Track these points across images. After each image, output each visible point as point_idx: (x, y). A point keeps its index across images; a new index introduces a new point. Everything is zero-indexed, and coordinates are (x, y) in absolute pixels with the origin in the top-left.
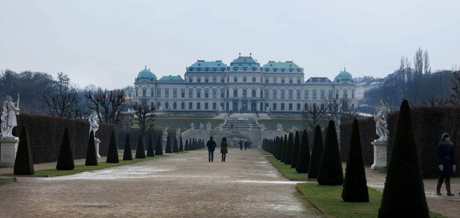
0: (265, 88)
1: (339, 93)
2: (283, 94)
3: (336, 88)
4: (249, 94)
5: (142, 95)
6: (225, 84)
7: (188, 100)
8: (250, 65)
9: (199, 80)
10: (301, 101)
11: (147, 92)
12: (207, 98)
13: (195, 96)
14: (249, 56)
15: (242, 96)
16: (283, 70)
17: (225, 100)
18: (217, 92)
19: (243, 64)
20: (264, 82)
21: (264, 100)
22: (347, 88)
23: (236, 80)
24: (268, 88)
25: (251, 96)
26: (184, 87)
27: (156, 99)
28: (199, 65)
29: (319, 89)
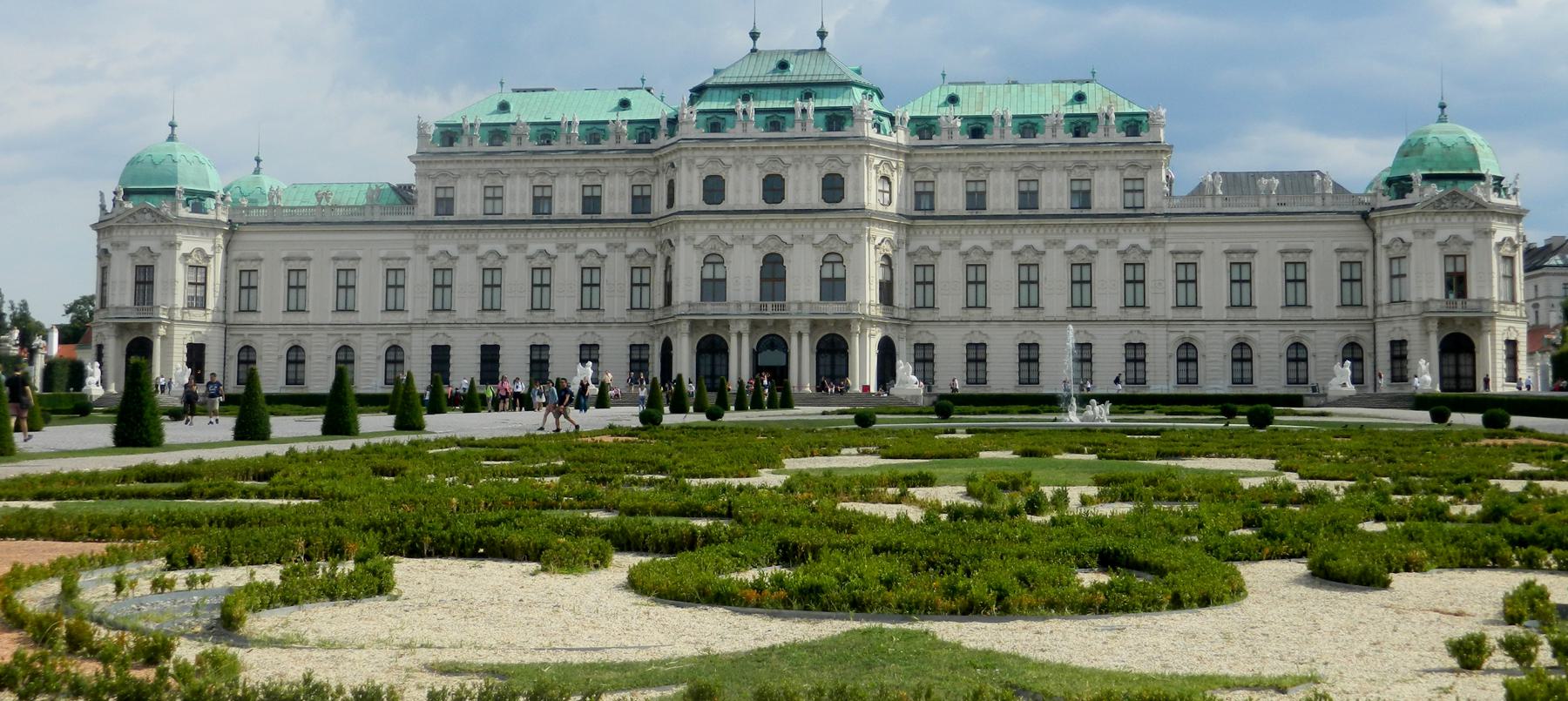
0: (915, 245)
1: (1412, 266)
2: (1029, 281)
3: (1390, 231)
7: (425, 325)
11: (158, 277)
12: (539, 316)
15: (754, 294)
16: (1029, 126)
17: (654, 325)
18: (606, 276)
21: (899, 323)
22: (1466, 234)
23: (714, 189)
24: (934, 245)
25: (814, 293)
26: (399, 243)
27: (226, 326)
28: (504, 107)
29: (1268, 247)
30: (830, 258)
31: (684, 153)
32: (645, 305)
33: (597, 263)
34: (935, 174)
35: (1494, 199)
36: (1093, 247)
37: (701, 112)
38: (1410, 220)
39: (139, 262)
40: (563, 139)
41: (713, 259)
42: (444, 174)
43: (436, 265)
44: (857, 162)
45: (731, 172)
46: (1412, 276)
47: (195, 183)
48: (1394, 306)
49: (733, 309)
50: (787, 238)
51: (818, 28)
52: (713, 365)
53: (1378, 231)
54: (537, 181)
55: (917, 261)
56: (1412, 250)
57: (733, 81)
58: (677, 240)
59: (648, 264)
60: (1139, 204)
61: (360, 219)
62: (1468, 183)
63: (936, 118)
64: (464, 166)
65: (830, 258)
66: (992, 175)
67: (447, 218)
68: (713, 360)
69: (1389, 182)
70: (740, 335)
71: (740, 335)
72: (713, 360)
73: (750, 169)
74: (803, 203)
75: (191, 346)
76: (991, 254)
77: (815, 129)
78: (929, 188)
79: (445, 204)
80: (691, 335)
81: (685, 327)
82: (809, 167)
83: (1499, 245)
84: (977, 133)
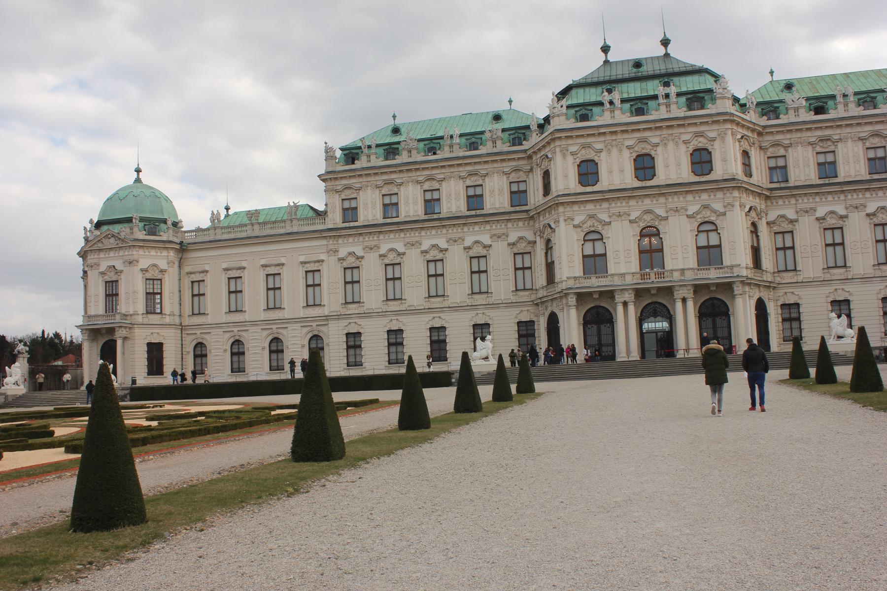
0: (772, 216)
4: (680, 256)
5: (101, 310)
6: (532, 217)
7: (339, 317)
8: (667, 84)
9: (390, 207)
11: (122, 289)
12: (436, 302)
13: (372, 293)
14: (661, 51)
15: (635, 266)
19: (624, 87)
20: (760, 177)
23: (588, 172)
24: (791, 214)
26: (316, 249)
27: (182, 327)
28: (396, 131)
30: (703, 228)
31: (558, 143)
32: (528, 286)
33: (483, 252)
34: (786, 148)
37: (569, 107)
39: (107, 278)
40: (447, 148)
41: (593, 236)
42: (348, 188)
43: (345, 264)
44: (722, 136)
45: (603, 155)
47: (150, 212)
49: (617, 281)
50: (661, 212)
51: (661, 37)
52: (599, 335)
54: (427, 186)
55: (776, 228)
57: (595, 80)
58: (557, 222)
59: (528, 249)
61: (282, 231)
63: (781, 101)
64: (364, 179)
65: (703, 228)
66: (839, 145)
67: (352, 224)
68: (599, 331)
70: (625, 304)
71: (625, 304)
72: (599, 331)
73: (620, 151)
74: (674, 178)
75: (150, 345)
76: (846, 217)
77: (679, 110)
78: (781, 162)
79: (350, 213)
80: (577, 307)
81: (572, 300)
82: (677, 144)
84: (819, 110)
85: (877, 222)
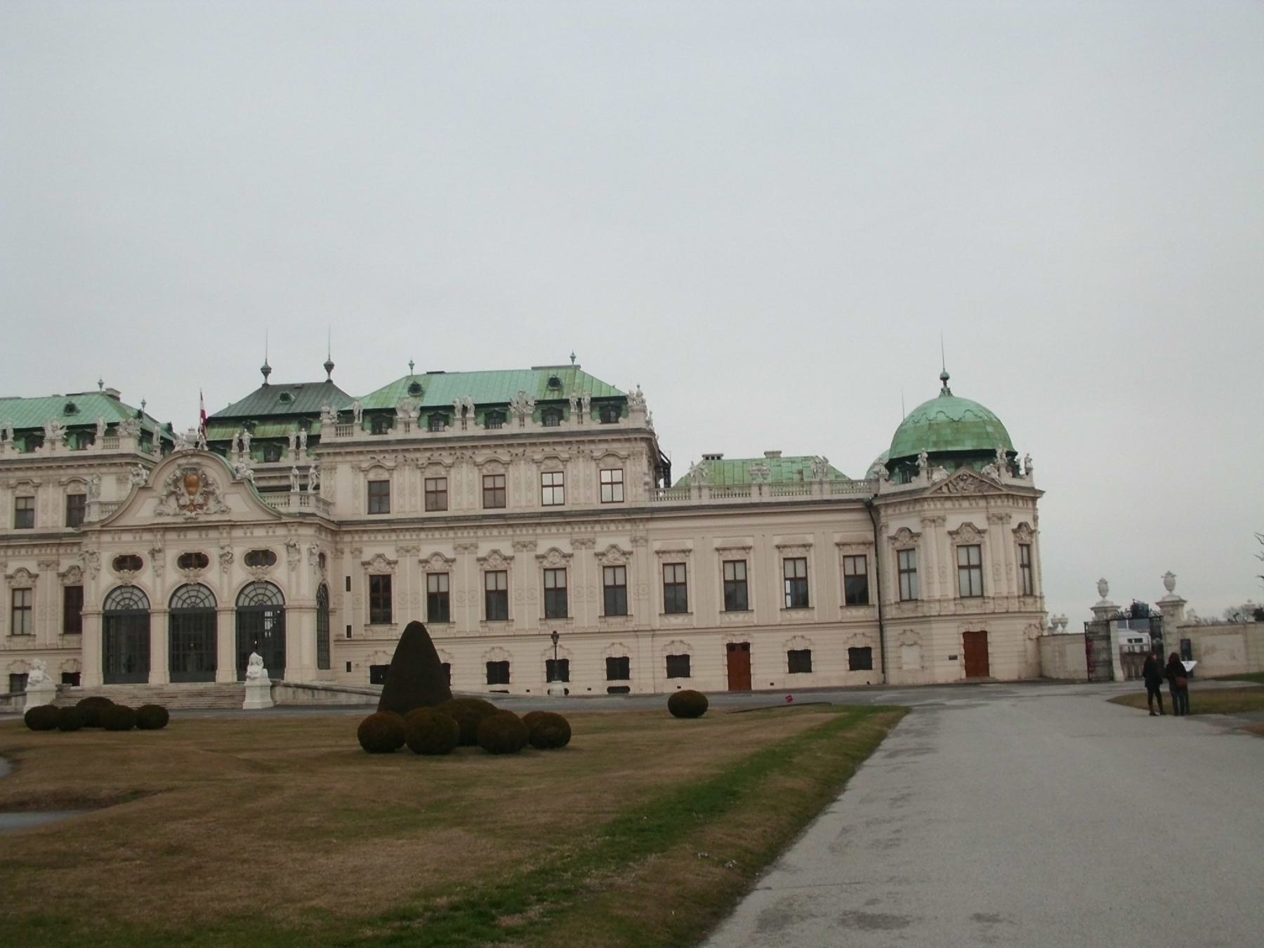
3: (893, 523)
10: (636, 633)
16: (494, 413)
22: (980, 521)
24: (391, 556)
29: (763, 544)
35: (1007, 478)
36: (567, 549)
38: (918, 507)
46: (922, 571)
48: (905, 606)
53: (883, 520)
56: (920, 541)
60: (618, 497)
62: (977, 466)
69: (892, 465)
83: (1014, 531)
85: (488, 568)
